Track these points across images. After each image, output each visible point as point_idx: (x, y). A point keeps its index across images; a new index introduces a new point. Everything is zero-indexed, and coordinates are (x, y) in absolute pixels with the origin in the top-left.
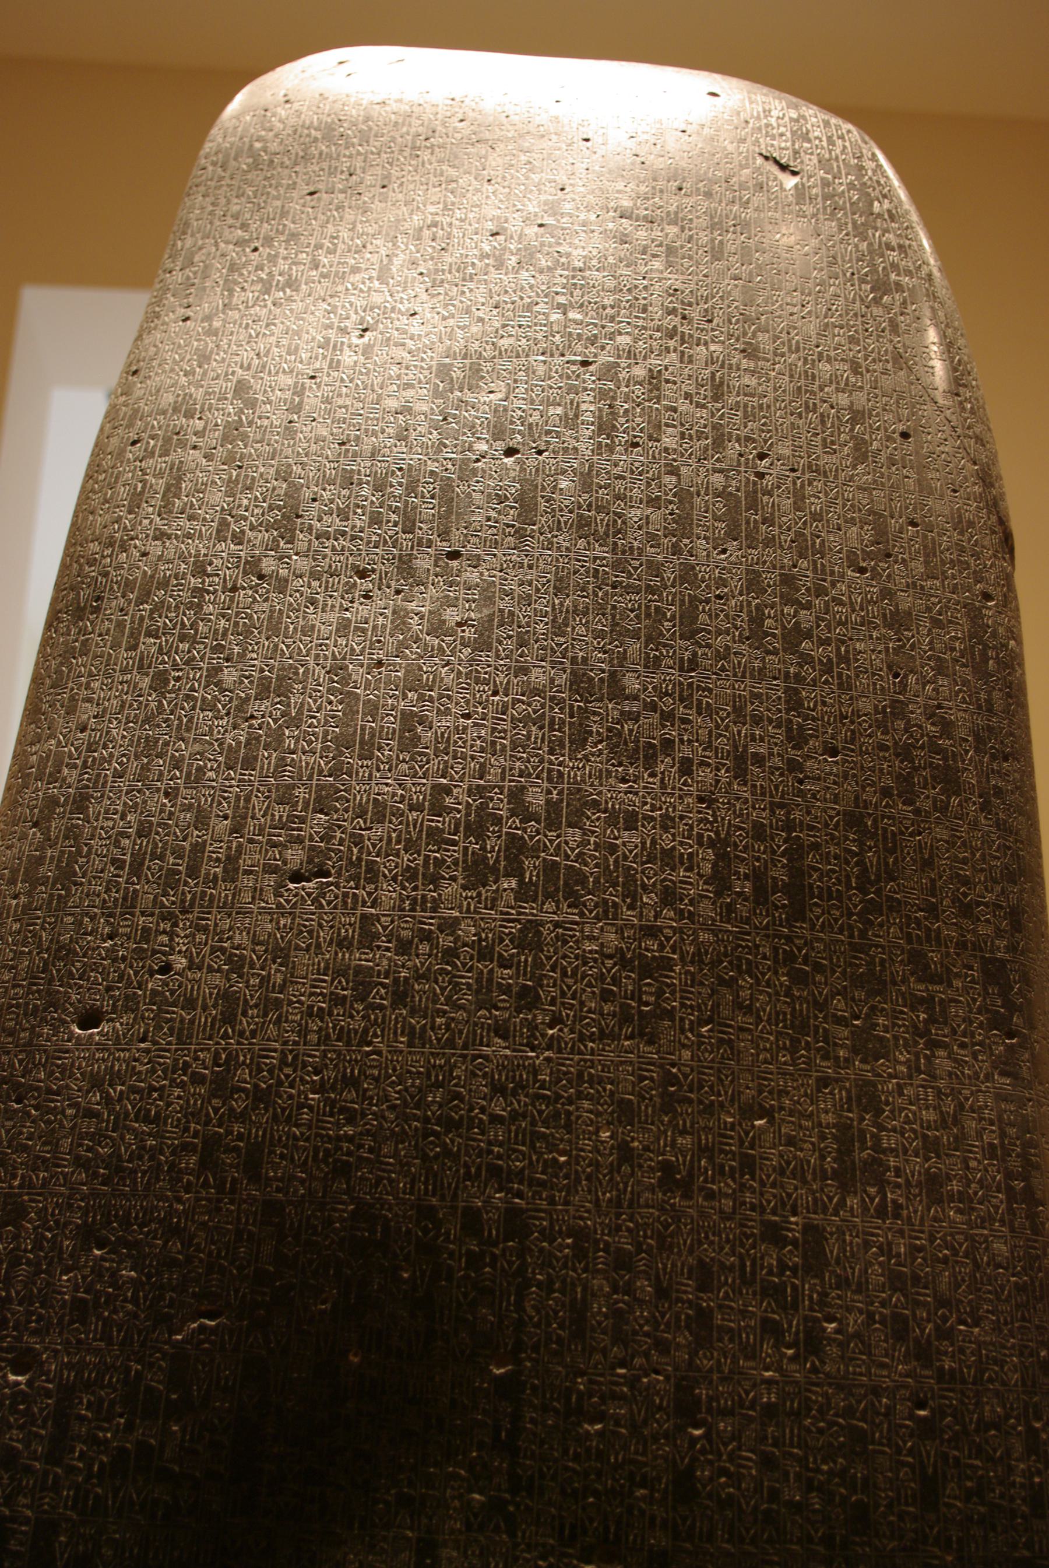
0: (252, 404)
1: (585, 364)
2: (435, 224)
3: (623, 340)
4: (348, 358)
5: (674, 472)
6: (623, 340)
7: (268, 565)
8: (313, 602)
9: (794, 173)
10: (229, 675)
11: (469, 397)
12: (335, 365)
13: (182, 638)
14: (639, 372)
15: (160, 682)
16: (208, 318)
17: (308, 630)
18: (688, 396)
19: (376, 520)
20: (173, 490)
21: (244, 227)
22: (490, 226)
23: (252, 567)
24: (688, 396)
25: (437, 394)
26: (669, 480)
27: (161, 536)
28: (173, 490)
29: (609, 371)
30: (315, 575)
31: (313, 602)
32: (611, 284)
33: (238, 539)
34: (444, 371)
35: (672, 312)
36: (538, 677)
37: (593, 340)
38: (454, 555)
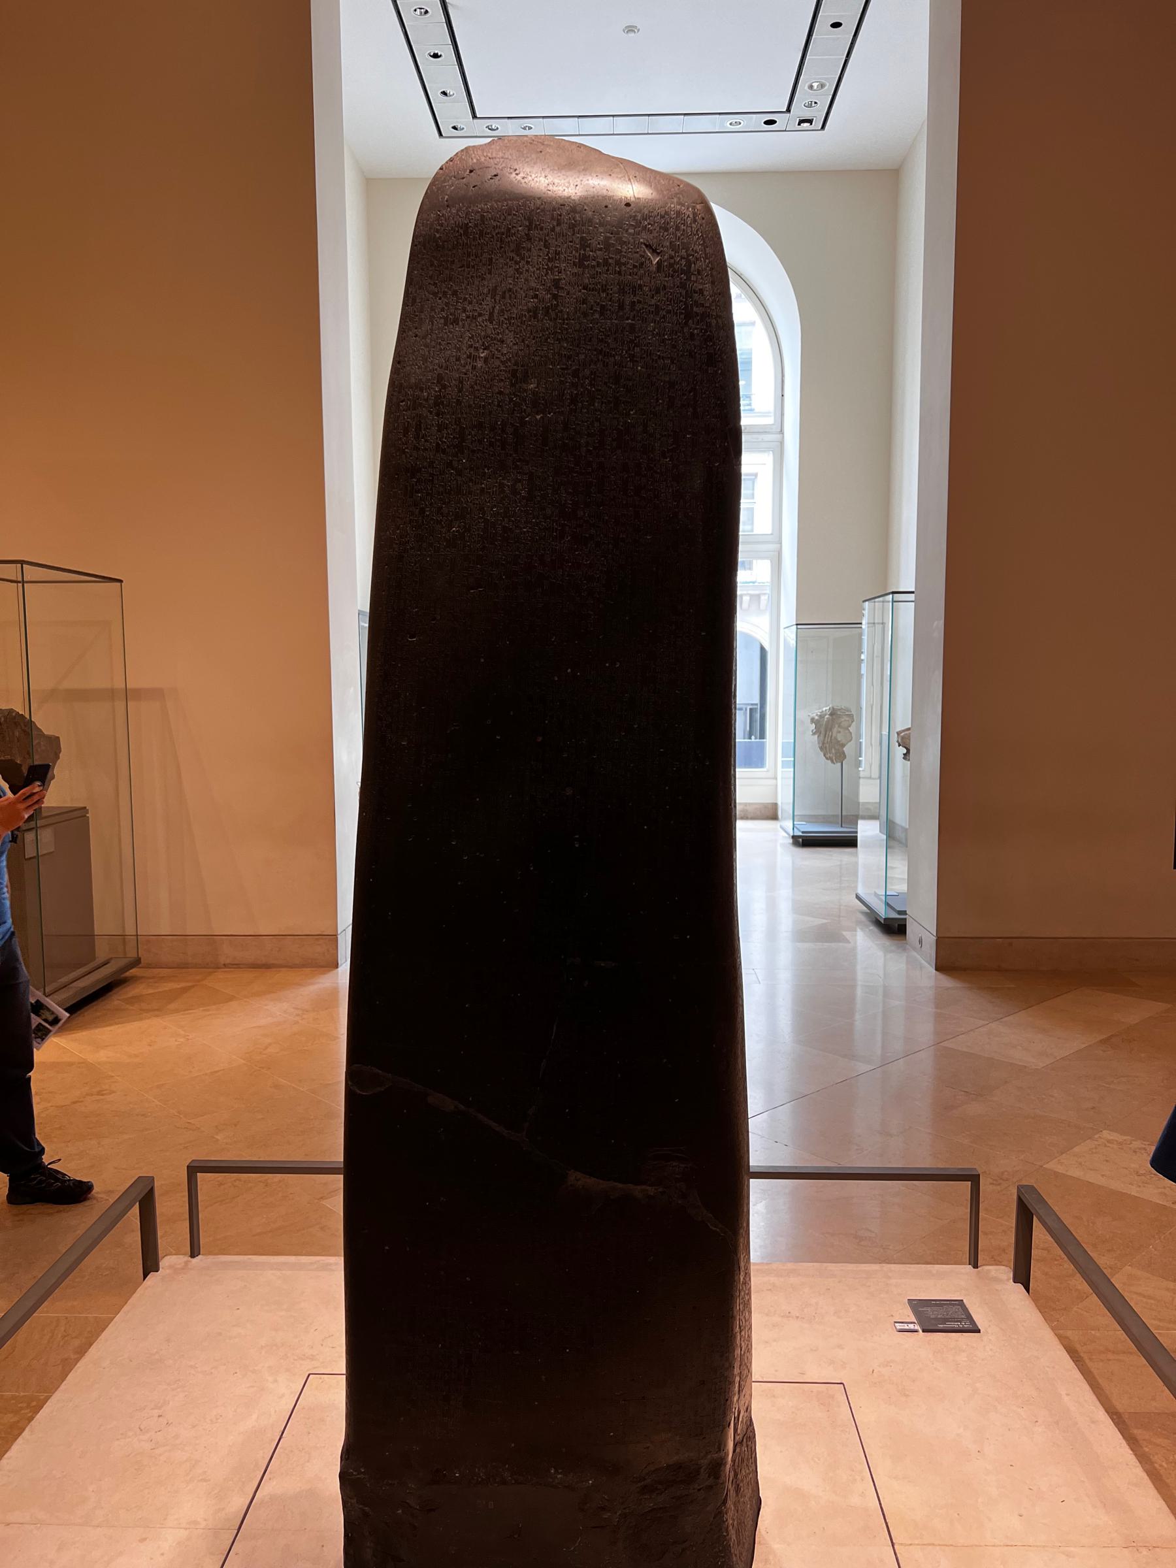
0: (444, 387)
1: (567, 369)
2: (510, 290)
3: (582, 357)
4: (479, 364)
5: (598, 420)
6: (582, 357)
7: (455, 464)
8: (471, 480)
9: (658, 254)
10: (445, 510)
11: (525, 386)
12: (474, 368)
13: (428, 494)
14: (587, 372)
15: (422, 511)
16: (424, 337)
17: (470, 493)
18: (605, 383)
19: (491, 444)
20: (418, 427)
21: (435, 284)
22: (531, 293)
23: (450, 465)
24: (605, 383)
25: (512, 385)
26: (596, 424)
27: (416, 448)
28: (418, 427)
29: (575, 374)
30: (472, 469)
31: (471, 480)
32: (577, 327)
33: (444, 451)
34: (514, 373)
35: (601, 341)
36: (549, 512)
37: (569, 357)
38: (520, 460)
